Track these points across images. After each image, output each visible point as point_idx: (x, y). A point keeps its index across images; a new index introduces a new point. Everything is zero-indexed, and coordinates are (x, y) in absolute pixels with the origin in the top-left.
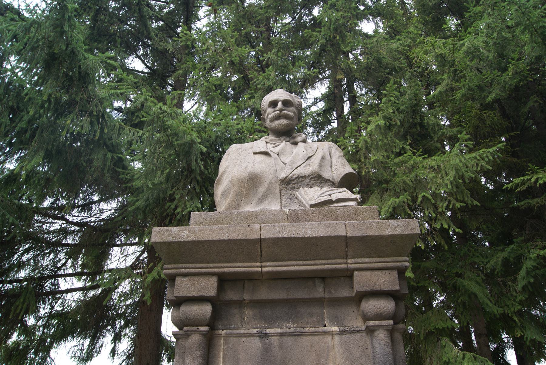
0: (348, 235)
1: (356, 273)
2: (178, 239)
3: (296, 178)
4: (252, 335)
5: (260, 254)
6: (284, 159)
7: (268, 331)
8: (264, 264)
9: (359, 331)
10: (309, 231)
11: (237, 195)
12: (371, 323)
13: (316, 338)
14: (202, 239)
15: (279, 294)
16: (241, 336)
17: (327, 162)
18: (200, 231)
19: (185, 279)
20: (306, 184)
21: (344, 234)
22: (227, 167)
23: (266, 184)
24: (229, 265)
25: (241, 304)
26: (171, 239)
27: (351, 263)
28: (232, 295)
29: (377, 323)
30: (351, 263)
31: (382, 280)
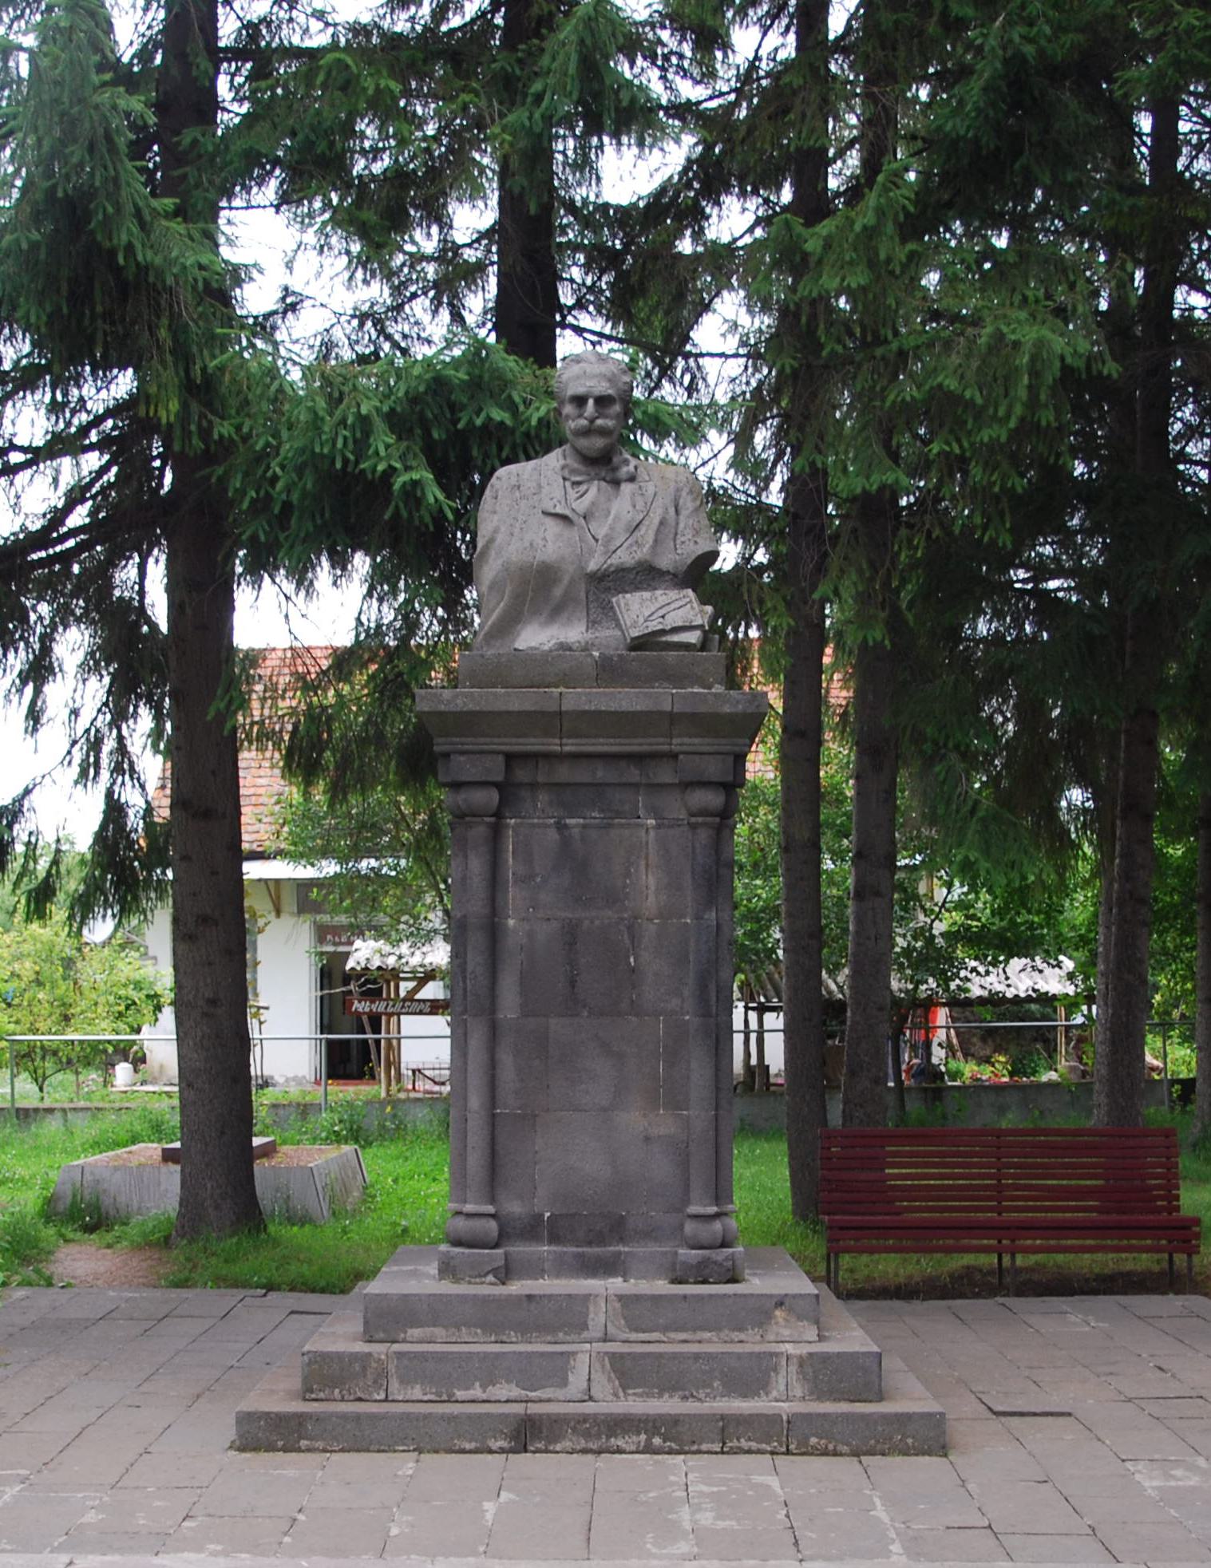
2: (452, 708)
6: (593, 526)
7: (568, 821)
8: (565, 741)
12: (693, 820)
13: (627, 832)
16: (533, 825)
19: (462, 758)
21: (668, 708)
22: (496, 531)
23: (565, 582)
24: (521, 740)
25: (533, 786)
26: (442, 708)
28: (522, 774)
29: (700, 819)
30: (677, 744)
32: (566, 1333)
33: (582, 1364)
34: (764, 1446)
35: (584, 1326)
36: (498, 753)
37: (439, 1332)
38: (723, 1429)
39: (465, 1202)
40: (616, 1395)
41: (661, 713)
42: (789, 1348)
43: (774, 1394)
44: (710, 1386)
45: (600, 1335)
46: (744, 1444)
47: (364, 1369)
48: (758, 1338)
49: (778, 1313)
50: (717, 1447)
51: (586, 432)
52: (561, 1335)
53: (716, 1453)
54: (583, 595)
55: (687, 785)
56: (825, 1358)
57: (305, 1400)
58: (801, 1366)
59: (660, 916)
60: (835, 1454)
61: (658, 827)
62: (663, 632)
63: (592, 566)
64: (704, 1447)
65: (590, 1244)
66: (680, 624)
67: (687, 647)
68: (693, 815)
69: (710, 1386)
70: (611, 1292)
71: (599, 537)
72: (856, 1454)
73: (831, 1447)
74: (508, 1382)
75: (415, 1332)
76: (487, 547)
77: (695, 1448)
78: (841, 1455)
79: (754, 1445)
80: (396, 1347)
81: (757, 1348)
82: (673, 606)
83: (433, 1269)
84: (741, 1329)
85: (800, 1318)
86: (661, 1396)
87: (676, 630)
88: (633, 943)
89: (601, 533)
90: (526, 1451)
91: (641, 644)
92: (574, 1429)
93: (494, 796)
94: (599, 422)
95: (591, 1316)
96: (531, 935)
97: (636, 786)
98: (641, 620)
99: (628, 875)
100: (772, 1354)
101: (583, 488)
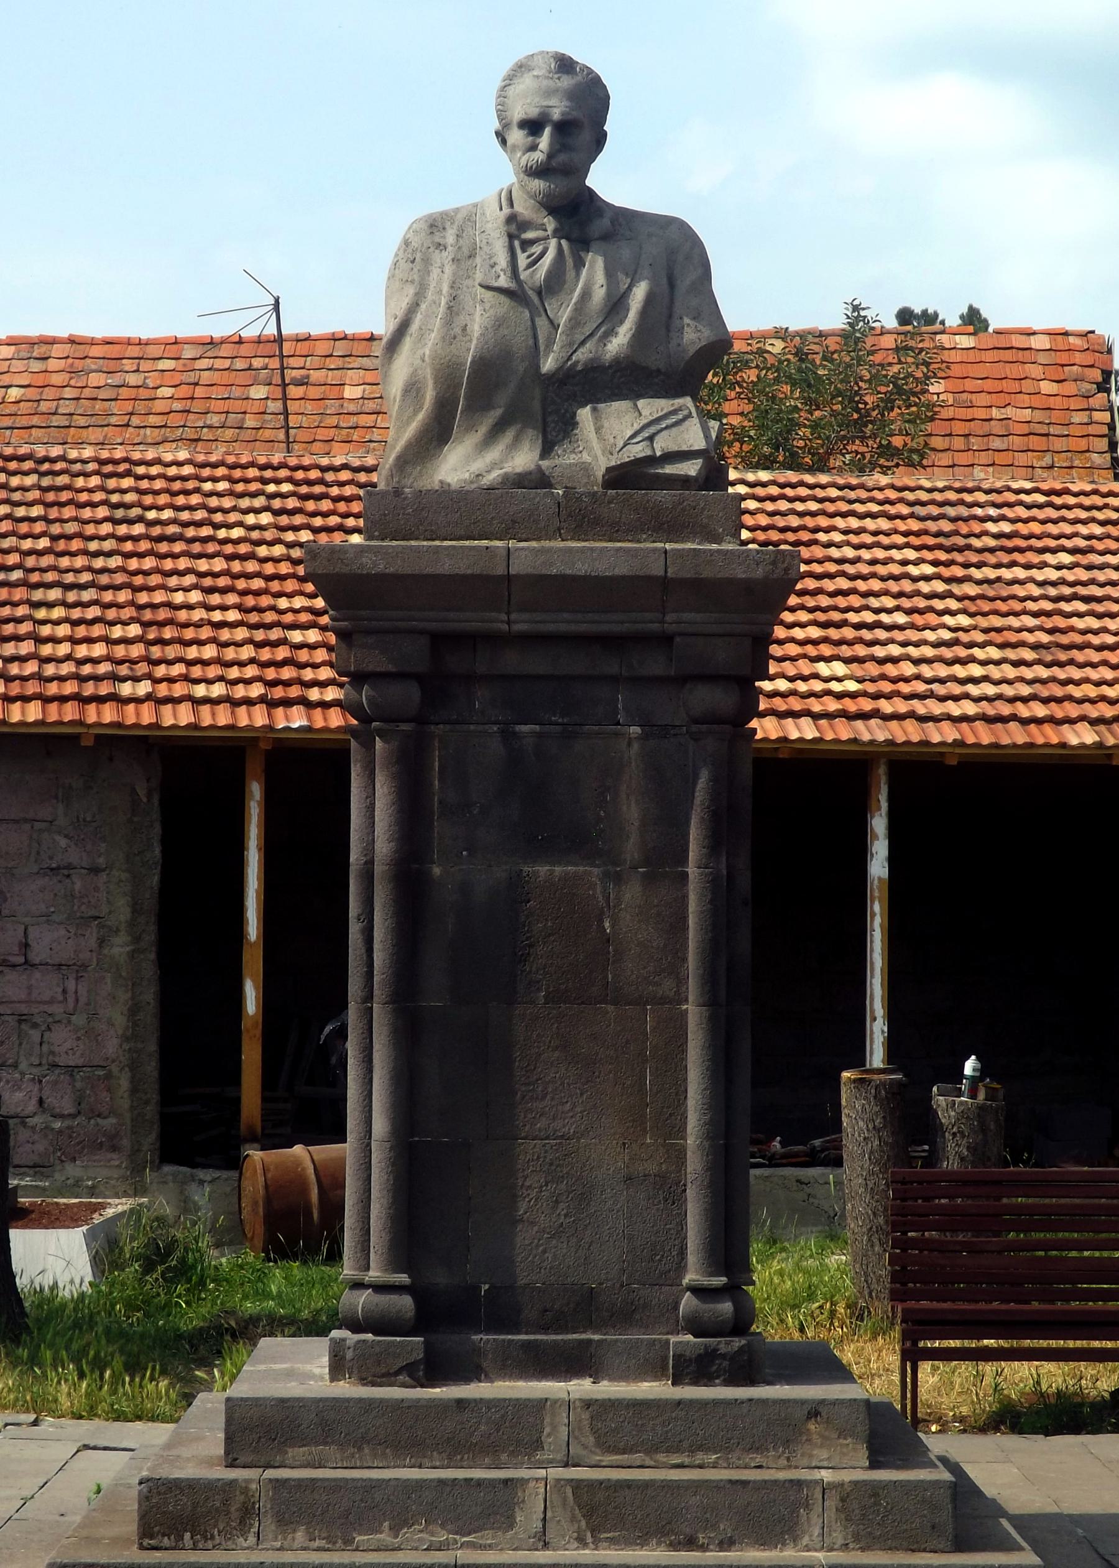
0: (670, 573)
5: (506, 598)
12: (694, 728)
14: (401, 571)
15: (538, 663)
21: (662, 573)
29: (704, 727)
35: (538, 1445)
36: (422, 632)
37: (331, 1451)
41: (649, 579)
42: (826, 1475)
43: (806, 1540)
45: (560, 1456)
47: (226, 1502)
48: (783, 1462)
49: (812, 1426)
54: (536, 405)
55: (682, 680)
57: (142, 1547)
61: (644, 737)
62: (651, 460)
67: (685, 482)
68: (696, 721)
75: (296, 1453)
80: (271, 1473)
81: (782, 1475)
83: (321, 1365)
85: (842, 1434)
93: (413, 692)
94: (562, 158)
97: (615, 680)
100: (799, 1484)
101: (537, 249)
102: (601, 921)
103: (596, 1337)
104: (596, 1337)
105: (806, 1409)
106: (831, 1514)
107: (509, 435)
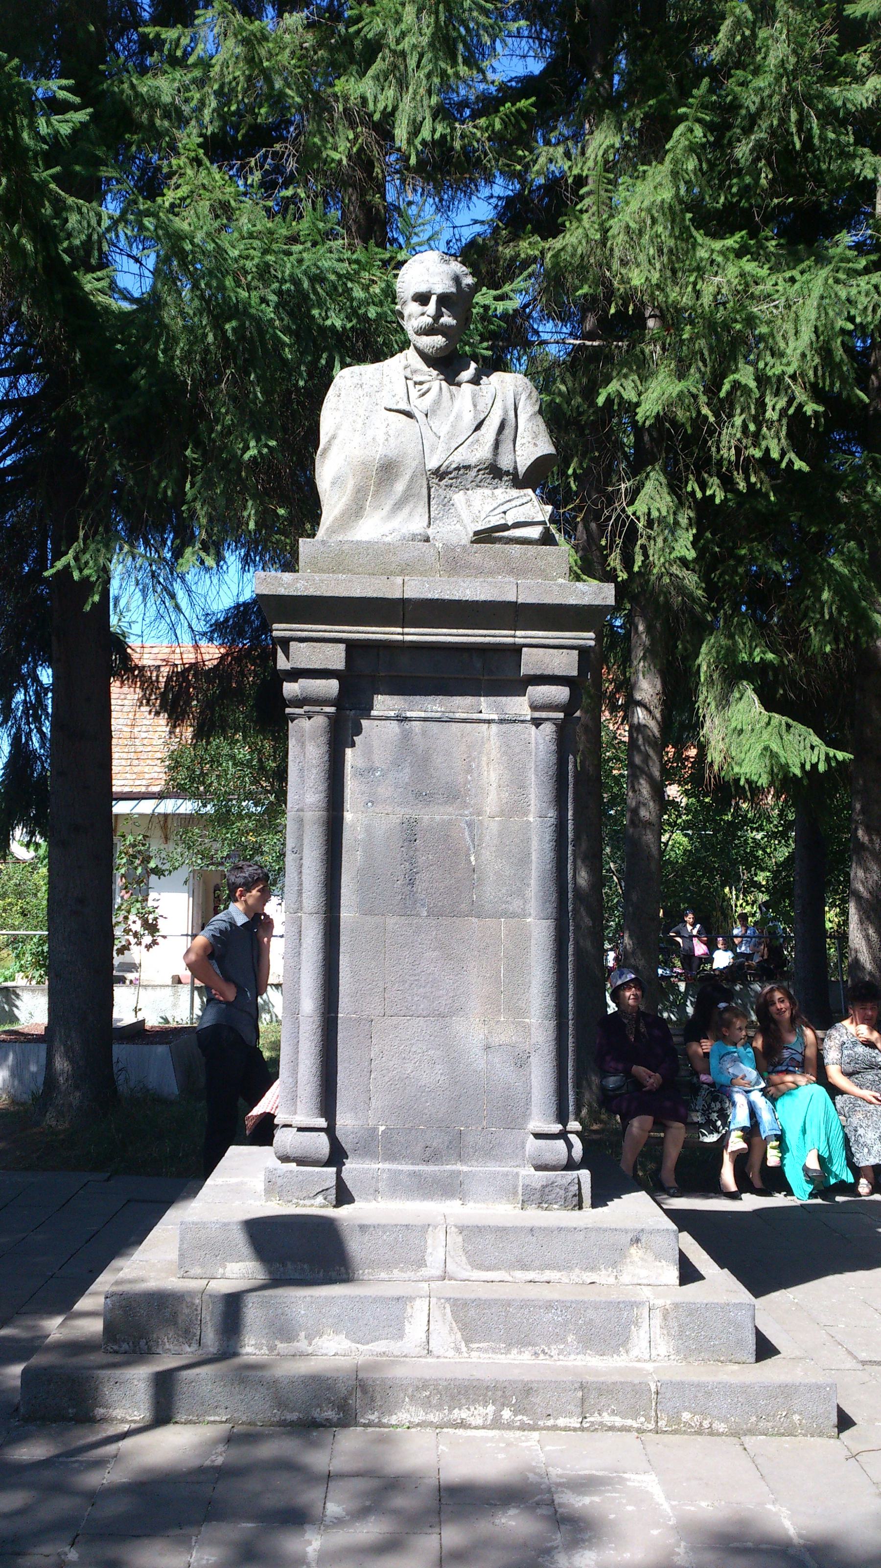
1: (524, 650)
3: (455, 469)
4: (387, 718)
6: (435, 423)
9: (523, 721)
10: (468, 592)
11: (358, 491)
12: (537, 715)
17: (508, 431)
18: (322, 581)
20: (470, 479)
21: (514, 600)
27: (521, 636)
29: (544, 715)
31: (556, 662)
32: (402, 1270)
33: (418, 1311)
34: (629, 1422)
35: (421, 1263)
38: (583, 1400)
39: (295, 1113)
40: (458, 1350)
44: (563, 1340)
45: (439, 1272)
46: (608, 1419)
49: (633, 1250)
50: (575, 1422)
51: (429, 331)
52: (395, 1271)
53: (575, 1430)
56: (692, 1310)
58: (665, 1318)
59: (502, 813)
60: (712, 1433)
62: (505, 527)
63: (433, 463)
64: (562, 1422)
65: (427, 1161)
66: (522, 520)
69: (563, 1340)
70: (451, 1221)
71: (442, 435)
72: (736, 1433)
73: (706, 1424)
74: (336, 1332)
76: (329, 443)
77: (550, 1423)
78: (720, 1435)
79: (618, 1421)
82: (514, 503)
84: (593, 1269)
85: (658, 1257)
86: (508, 1352)
87: (518, 525)
88: (473, 841)
89: (443, 431)
90: (356, 1424)
91: (485, 536)
92: (412, 1398)
95: (429, 1250)
96: (368, 829)
98: (483, 515)
99: (469, 771)
101: (425, 387)
102: (468, 855)
103: (465, 1168)
104: (465, 1168)
105: (630, 1236)
106: (657, 1331)
107: (406, 511)
